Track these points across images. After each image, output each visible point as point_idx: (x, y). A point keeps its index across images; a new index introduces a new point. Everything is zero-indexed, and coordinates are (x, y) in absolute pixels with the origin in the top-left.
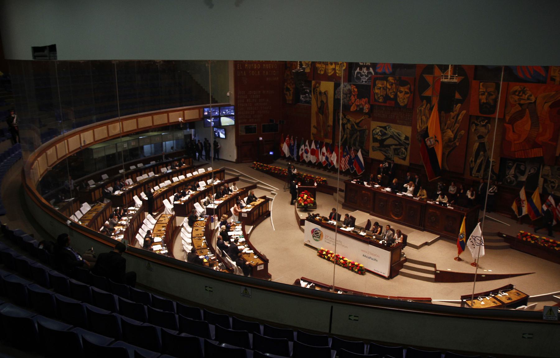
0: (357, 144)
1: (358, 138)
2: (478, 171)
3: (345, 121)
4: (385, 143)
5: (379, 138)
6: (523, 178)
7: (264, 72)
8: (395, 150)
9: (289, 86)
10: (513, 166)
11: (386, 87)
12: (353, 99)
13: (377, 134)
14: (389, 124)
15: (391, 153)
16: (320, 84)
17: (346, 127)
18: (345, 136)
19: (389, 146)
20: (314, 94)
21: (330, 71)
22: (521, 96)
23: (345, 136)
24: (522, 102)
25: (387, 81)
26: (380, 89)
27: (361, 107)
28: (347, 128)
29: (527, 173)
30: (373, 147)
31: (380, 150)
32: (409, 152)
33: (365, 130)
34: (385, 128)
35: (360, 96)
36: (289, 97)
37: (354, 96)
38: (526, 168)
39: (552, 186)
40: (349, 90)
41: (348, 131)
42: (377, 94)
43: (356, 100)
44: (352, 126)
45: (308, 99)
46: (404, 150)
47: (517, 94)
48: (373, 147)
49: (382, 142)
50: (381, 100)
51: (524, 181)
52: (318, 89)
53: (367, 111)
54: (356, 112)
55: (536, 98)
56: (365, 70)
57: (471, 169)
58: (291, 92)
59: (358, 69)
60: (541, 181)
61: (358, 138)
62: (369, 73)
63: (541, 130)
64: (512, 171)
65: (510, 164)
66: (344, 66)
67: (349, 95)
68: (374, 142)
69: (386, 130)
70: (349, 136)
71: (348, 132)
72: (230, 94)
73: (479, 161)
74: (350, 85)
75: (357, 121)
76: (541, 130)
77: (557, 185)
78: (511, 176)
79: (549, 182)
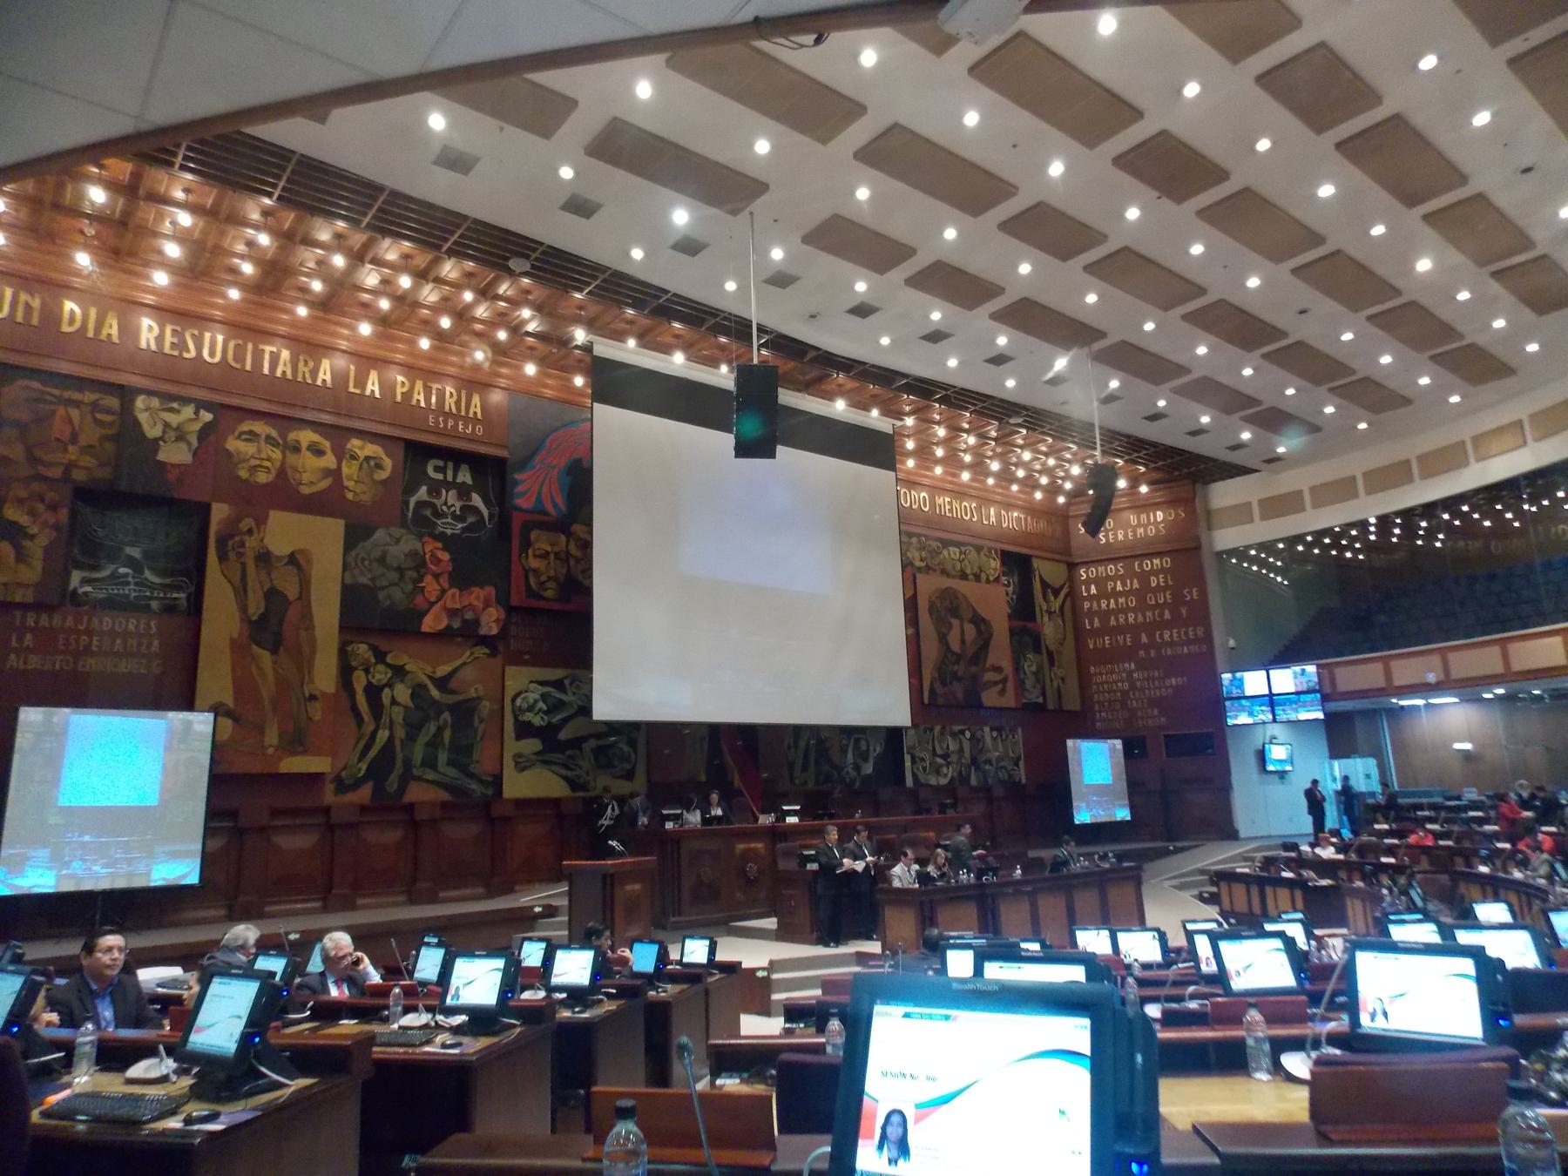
0: (443, 757)
1: (447, 734)
2: (805, 769)
3: (381, 675)
4: (563, 736)
5: (537, 721)
8: (598, 751)
11: (568, 553)
12: (431, 586)
13: (531, 708)
14: (570, 671)
15: (586, 763)
16: (261, 521)
18: (383, 735)
19: (577, 743)
20: (222, 557)
21: (306, 478)
23: (383, 735)
25: (569, 534)
26: (546, 555)
27: (469, 616)
28: (394, 702)
29: (873, 755)
30: (518, 756)
31: (546, 763)
32: (641, 749)
33: (479, 698)
34: (558, 685)
35: (462, 578)
37: (436, 576)
40: (413, 554)
41: (398, 714)
42: (536, 572)
43: (444, 591)
44: (418, 691)
45: (131, 591)
46: (626, 748)
49: (547, 735)
50: (549, 594)
51: (869, 776)
52: (251, 543)
53: (494, 631)
56: (451, 497)
57: (791, 766)
59: (424, 489)
60: (908, 758)
61: (447, 734)
62: (469, 509)
64: (850, 755)
66: (379, 466)
67: (415, 575)
70: (400, 733)
73: (802, 744)
74: (420, 537)
75: (443, 670)
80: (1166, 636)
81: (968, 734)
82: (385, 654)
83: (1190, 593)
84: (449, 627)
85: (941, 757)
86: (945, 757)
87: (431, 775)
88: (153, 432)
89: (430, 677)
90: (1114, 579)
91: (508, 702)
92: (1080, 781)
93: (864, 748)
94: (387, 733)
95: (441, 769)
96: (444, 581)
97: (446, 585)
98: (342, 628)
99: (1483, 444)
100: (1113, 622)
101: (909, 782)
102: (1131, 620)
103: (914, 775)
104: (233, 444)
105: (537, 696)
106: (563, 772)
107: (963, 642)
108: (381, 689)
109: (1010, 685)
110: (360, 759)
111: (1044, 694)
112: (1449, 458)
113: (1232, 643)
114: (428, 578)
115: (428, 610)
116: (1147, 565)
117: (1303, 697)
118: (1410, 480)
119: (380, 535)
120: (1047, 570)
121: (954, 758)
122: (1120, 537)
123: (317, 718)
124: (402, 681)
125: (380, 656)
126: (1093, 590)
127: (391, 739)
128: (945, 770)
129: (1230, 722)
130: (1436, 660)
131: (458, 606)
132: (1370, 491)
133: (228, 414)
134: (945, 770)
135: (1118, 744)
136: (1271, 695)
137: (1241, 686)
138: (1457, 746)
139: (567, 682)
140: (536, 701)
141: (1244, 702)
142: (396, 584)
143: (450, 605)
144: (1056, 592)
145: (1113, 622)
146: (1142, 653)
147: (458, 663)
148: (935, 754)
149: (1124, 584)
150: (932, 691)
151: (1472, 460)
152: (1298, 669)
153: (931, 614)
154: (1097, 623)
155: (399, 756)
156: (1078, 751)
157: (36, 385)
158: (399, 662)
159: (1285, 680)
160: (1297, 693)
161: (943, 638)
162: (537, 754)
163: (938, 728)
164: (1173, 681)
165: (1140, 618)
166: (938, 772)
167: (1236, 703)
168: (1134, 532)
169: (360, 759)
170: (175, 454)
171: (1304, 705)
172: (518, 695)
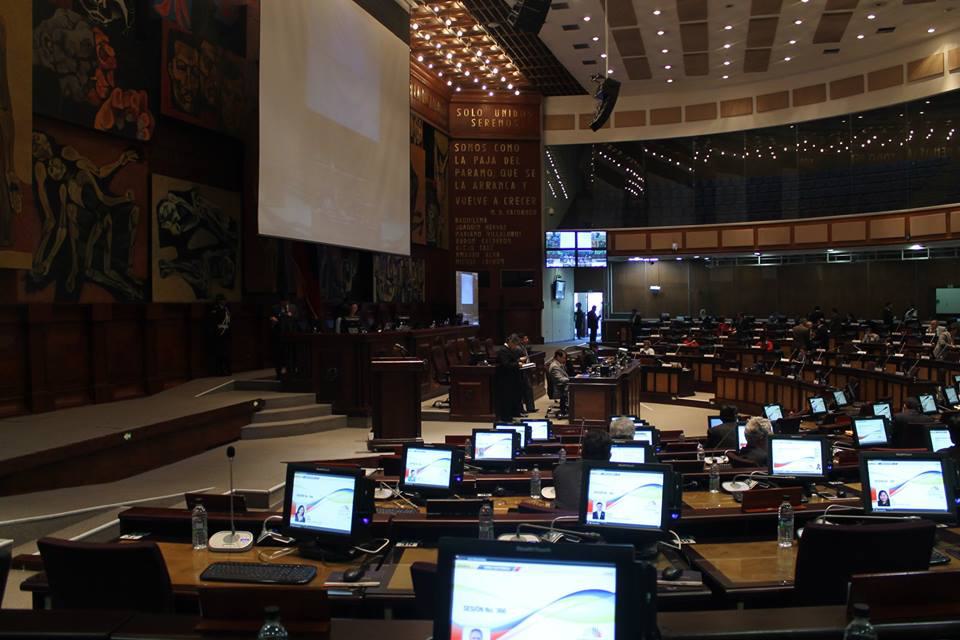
0: (107, 260)
1: (110, 235)
5: (174, 229)
13: (170, 216)
17: (63, 199)
18: (62, 233)
23: (62, 233)
27: (129, 118)
28: (69, 201)
29: (352, 275)
31: (181, 271)
34: (186, 196)
37: (105, 71)
41: (72, 212)
43: (111, 89)
44: (87, 190)
46: (230, 261)
48: (162, 262)
50: (187, 106)
53: (147, 138)
54: (109, 135)
60: (375, 279)
61: (110, 235)
68: (161, 247)
69: (192, 205)
70: (75, 234)
71: (74, 219)
75: (104, 172)
80: (511, 202)
82: (61, 147)
83: (530, 172)
84: (115, 126)
86: (391, 280)
87: (99, 279)
89: (96, 178)
90: (480, 154)
91: (154, 210)
92: (460, 301)
94: (65, 231)
95: (107, 272)
96: (110, 75)
97: (113, 84)
98: (34, 114)
99: (728, 108)
100: (475, 187)
102: (488, 186)
105: (174, 207)
106: (190, 279)
108: (61, 182)
109: (424, 227)
110: (45, 258)
111: (436, 236)
112: (704, 112)
113: (551, 211)
114: (99, 72)
115: (101, 106)
116: (503, 148)
117: (597, 252)
118: (680, 121)
119: (59, 14)
120: (440, 140)
121: (395, 282)
122: (486, 124)
123: (19, 211)
124: (74, 178)
125: (57, 150)
126: (463, 161)
127: (68, 236)
129: (548, 265)
130: (680, 234)
131: (121, 107)
132: (654, 123)
135: (476, 274)
136: (576, 249)
137: (558, 242)
138: (652, 288)
139: (193, 194)
140: (173, 211)
141: (559, 252)
142: (74, 74)
143: (115, 105)
144: (443, 158)
145: (475, 187)
146: (493, 211)
147: (117, 165)
149: (485, 160)
151: (719, 116)
152: (595, 233)
154: (463, 186)
155: (75, 258)
156: (460, 277)
158: (74, 160)
159: (586, 239)
160: (593, 249)
162: (174, 261)
164: (513, 233)
165: (494, 187)
166: (388, 293)
167: (554, 252)
168: (497, 121)
169: (45, 258)
171: (596, 257)
172: (162, 202)
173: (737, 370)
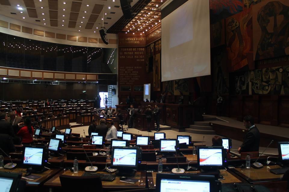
0: (170, 89)
6: (244, 88)
7: (135, 56)
9: (147, 63)
10: (238, 80)
16: (156, 56)
22: (232, 25)
24: (233, 29)
36: (147, 69)
38: (245, 78)
39: (256, 87)
47: (230, 24)
48: (175, 87)
55: (239, 23)
58: (148, 66)
63: (244, 44)
64: (238, 84)
65: (237, 79)
68: (175, 84)
72: (116, 68)
76: (244, 44)
77: (259, 85)
78: (238, 88)
79: (255, 84)
81: (281, 70)
85: (265, 82)
86: (267, 82)
87: (169, 91)
88: (151, 49)
93: (243, 80)
101: (250, 93)
103: (253, 91)
104: (156, 46)
107: (275, 25)
128: (267, 88)
133: (155, 43)
134: (267, 88)
148: (262, 81)
150: (257, 54)
153: (258, 19)
157: (148, 47)
161: (264, 29)
163: (264, 70)
166: (263, 89)
170: (152, 51)
173: (66, 116)
